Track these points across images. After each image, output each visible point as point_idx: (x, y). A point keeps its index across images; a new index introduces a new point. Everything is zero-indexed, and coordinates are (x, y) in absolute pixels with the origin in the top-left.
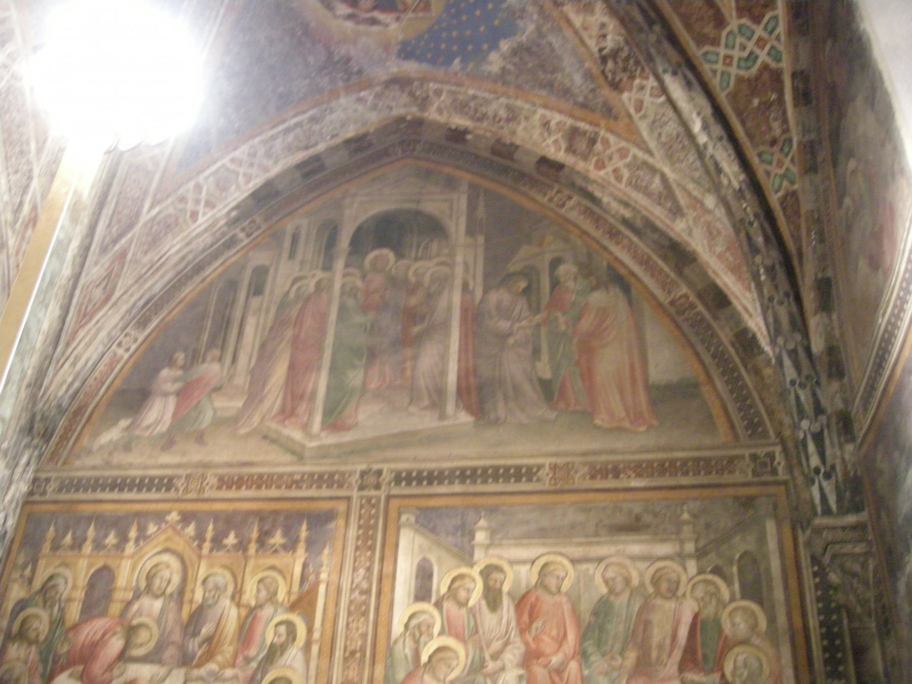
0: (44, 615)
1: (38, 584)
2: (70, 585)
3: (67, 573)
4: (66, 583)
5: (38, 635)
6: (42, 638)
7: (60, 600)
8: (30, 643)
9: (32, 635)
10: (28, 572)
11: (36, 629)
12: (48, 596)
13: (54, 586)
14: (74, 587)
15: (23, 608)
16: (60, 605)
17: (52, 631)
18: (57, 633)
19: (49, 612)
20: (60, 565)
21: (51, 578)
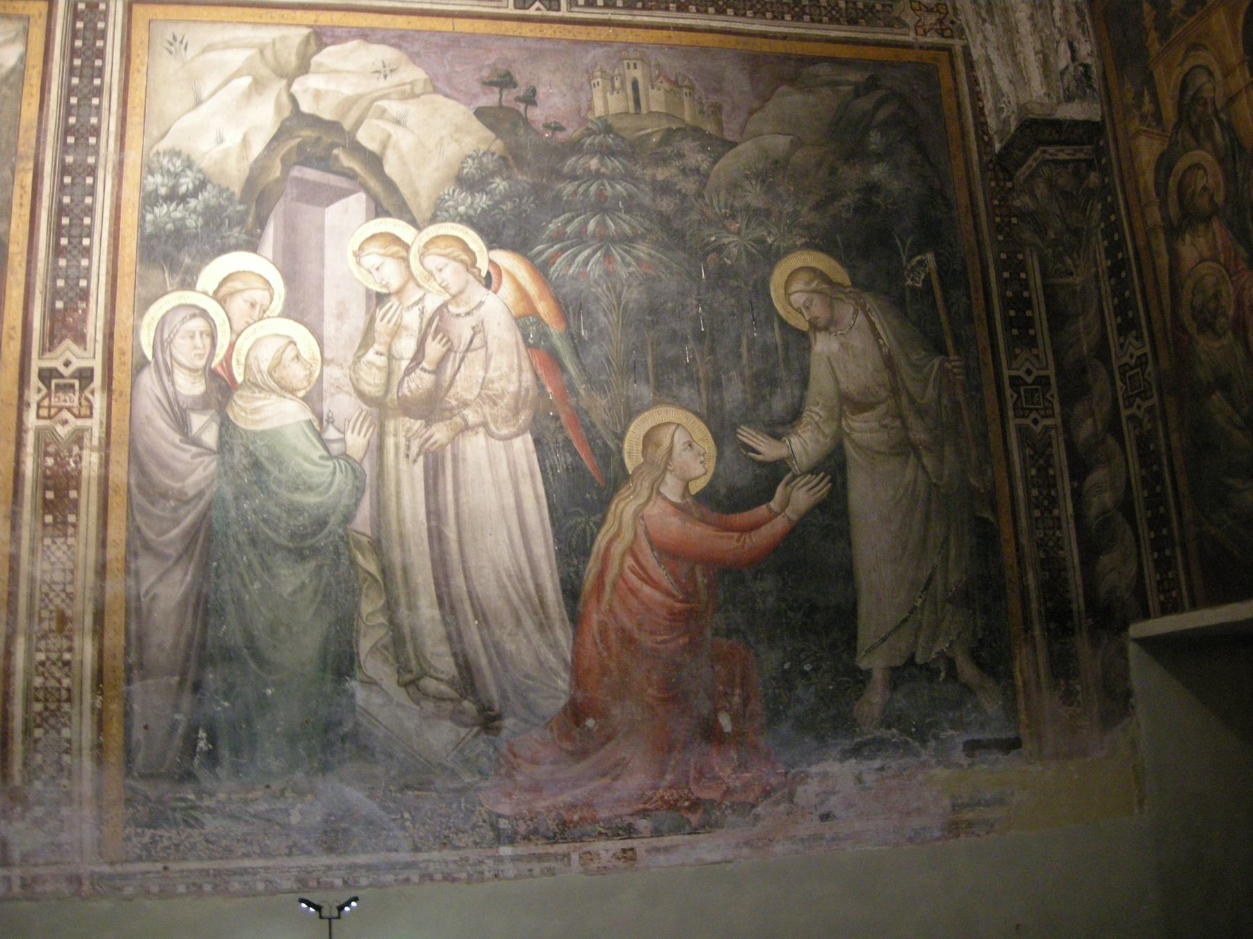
0: (1203, 156)
1: (1169, 112)
2: (1218, 74)
3: (1204, 57)
4: (1211, 74)
5: (1211, 200)
6: (1219, 198)
7: (1216, 112)
8: (1207, 219)
9: (1203, 203)
10: (1148, 107)
11: (1205, 188)
12: (1194, 120)
13: (1195, 98)
14: (1227, 74)
15: (1169, 171)
16: (1219, 120)
17: (1231, 177)
18: (1240, 175)
19: (1208, 145)
20: (1186, 57)
21: (1184, 88)
